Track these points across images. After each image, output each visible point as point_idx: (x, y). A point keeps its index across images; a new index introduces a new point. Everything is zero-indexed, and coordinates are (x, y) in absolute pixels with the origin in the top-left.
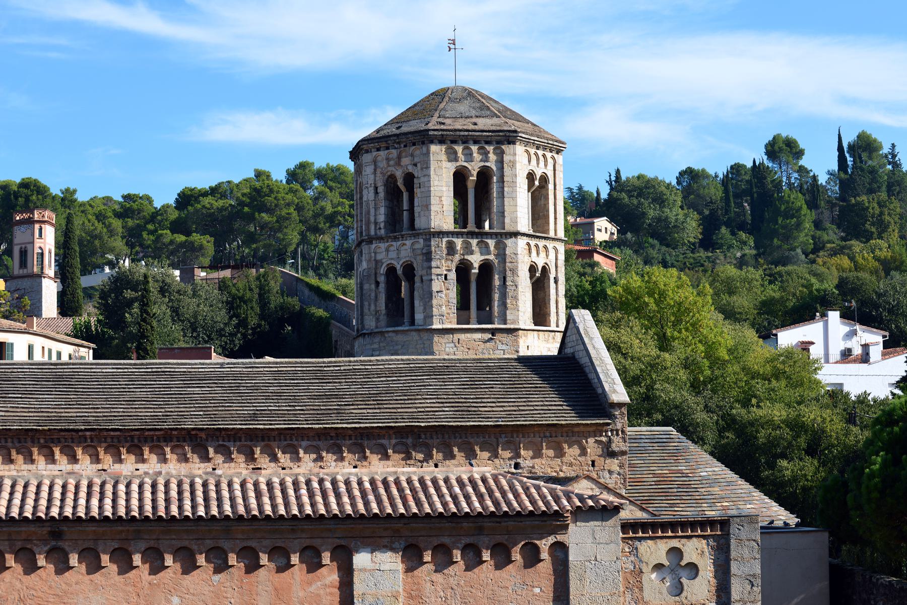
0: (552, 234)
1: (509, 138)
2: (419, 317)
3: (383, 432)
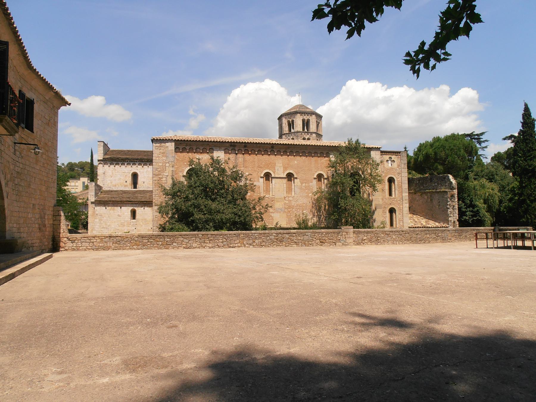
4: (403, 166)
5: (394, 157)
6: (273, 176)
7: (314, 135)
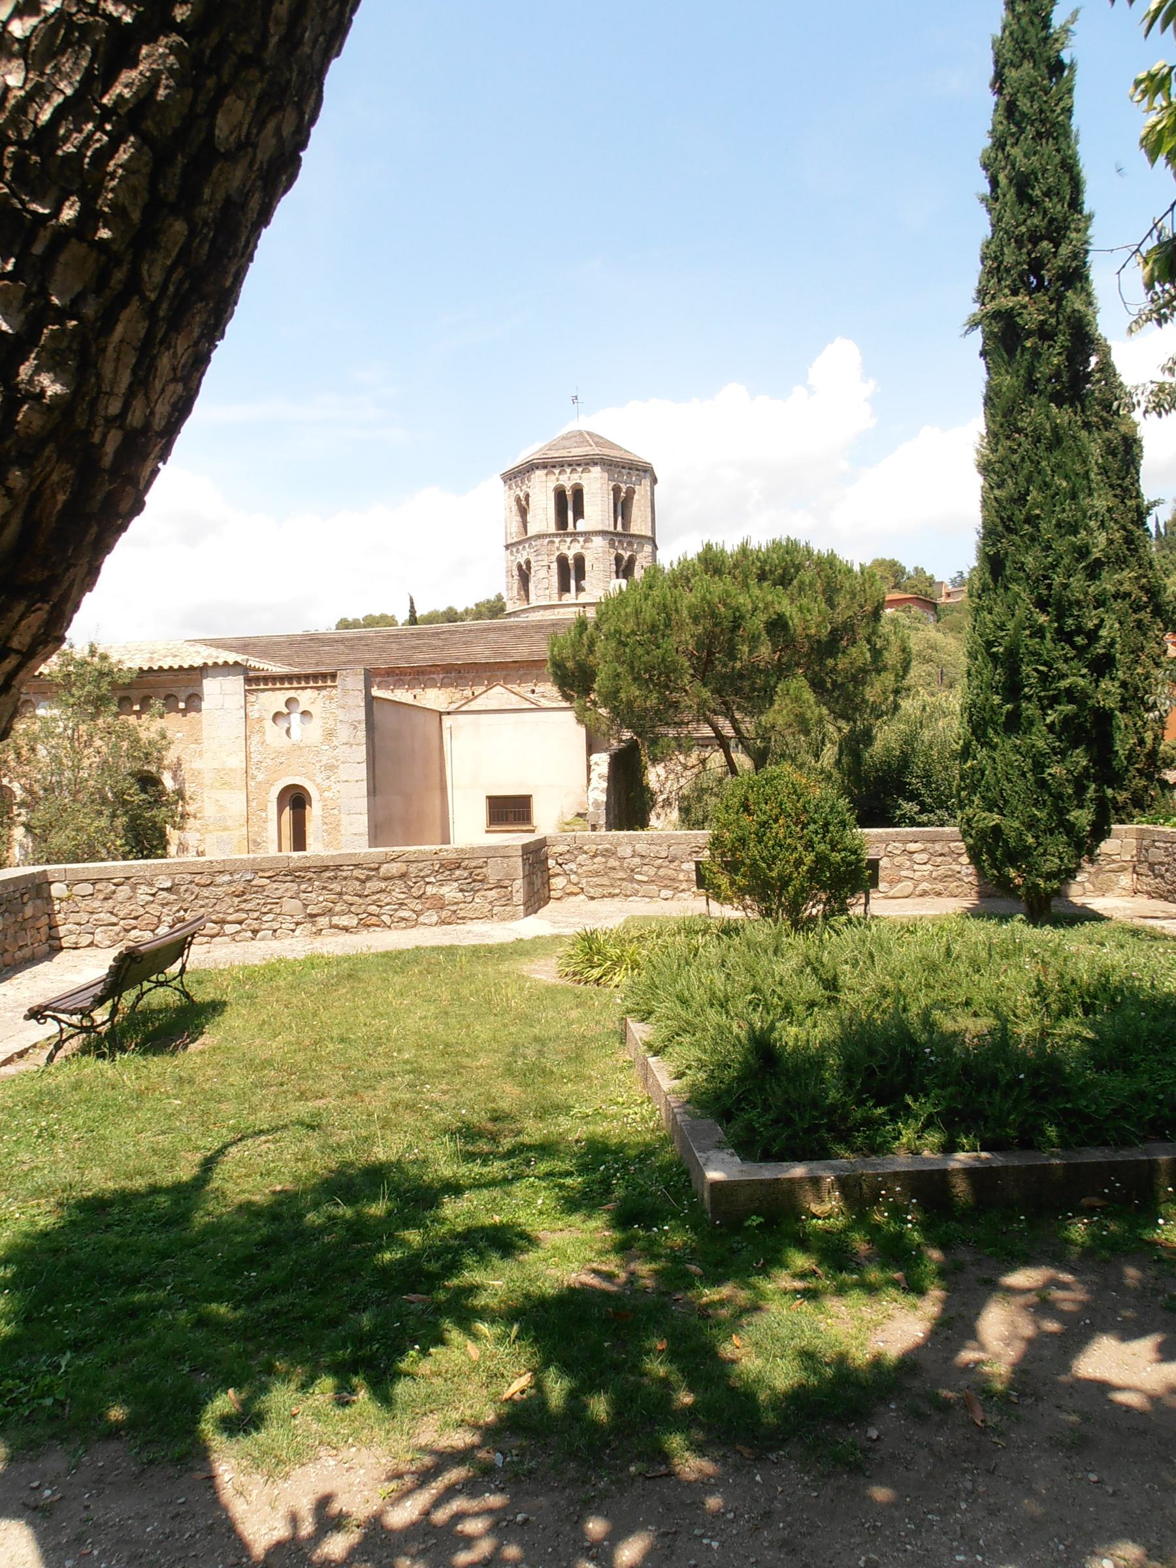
3: (433, 669)
4: (344, 733)
5: (307, 697)
7: (598, 542)
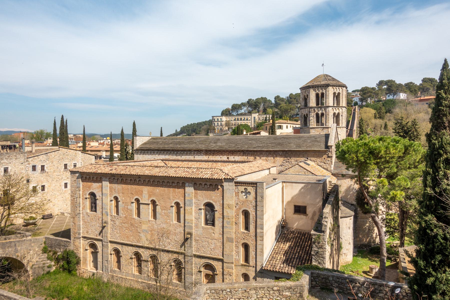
0: (341, 105)
1: (327, 86)
2: (308, 125)
5: (250, 189)
6: (141, 202)
